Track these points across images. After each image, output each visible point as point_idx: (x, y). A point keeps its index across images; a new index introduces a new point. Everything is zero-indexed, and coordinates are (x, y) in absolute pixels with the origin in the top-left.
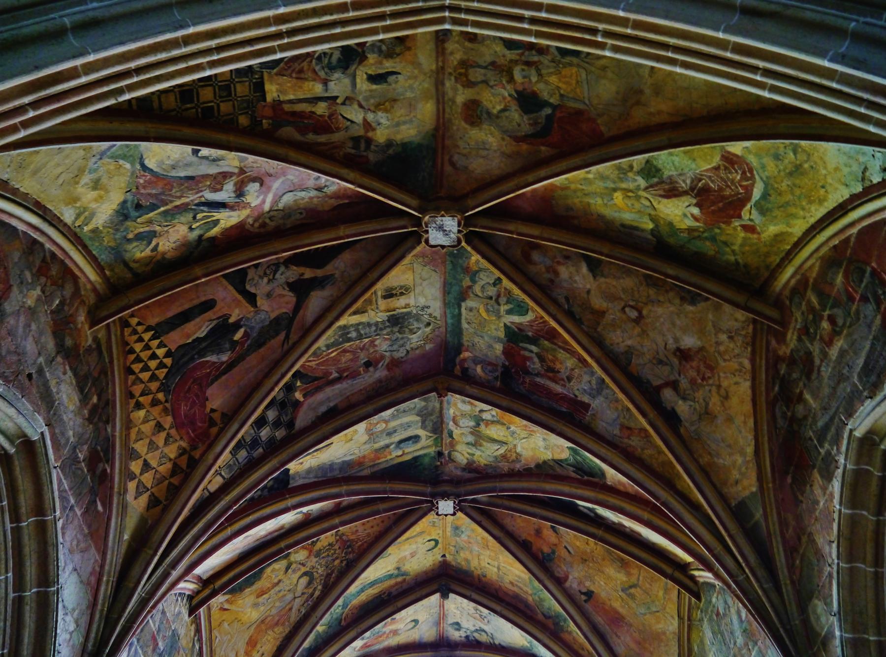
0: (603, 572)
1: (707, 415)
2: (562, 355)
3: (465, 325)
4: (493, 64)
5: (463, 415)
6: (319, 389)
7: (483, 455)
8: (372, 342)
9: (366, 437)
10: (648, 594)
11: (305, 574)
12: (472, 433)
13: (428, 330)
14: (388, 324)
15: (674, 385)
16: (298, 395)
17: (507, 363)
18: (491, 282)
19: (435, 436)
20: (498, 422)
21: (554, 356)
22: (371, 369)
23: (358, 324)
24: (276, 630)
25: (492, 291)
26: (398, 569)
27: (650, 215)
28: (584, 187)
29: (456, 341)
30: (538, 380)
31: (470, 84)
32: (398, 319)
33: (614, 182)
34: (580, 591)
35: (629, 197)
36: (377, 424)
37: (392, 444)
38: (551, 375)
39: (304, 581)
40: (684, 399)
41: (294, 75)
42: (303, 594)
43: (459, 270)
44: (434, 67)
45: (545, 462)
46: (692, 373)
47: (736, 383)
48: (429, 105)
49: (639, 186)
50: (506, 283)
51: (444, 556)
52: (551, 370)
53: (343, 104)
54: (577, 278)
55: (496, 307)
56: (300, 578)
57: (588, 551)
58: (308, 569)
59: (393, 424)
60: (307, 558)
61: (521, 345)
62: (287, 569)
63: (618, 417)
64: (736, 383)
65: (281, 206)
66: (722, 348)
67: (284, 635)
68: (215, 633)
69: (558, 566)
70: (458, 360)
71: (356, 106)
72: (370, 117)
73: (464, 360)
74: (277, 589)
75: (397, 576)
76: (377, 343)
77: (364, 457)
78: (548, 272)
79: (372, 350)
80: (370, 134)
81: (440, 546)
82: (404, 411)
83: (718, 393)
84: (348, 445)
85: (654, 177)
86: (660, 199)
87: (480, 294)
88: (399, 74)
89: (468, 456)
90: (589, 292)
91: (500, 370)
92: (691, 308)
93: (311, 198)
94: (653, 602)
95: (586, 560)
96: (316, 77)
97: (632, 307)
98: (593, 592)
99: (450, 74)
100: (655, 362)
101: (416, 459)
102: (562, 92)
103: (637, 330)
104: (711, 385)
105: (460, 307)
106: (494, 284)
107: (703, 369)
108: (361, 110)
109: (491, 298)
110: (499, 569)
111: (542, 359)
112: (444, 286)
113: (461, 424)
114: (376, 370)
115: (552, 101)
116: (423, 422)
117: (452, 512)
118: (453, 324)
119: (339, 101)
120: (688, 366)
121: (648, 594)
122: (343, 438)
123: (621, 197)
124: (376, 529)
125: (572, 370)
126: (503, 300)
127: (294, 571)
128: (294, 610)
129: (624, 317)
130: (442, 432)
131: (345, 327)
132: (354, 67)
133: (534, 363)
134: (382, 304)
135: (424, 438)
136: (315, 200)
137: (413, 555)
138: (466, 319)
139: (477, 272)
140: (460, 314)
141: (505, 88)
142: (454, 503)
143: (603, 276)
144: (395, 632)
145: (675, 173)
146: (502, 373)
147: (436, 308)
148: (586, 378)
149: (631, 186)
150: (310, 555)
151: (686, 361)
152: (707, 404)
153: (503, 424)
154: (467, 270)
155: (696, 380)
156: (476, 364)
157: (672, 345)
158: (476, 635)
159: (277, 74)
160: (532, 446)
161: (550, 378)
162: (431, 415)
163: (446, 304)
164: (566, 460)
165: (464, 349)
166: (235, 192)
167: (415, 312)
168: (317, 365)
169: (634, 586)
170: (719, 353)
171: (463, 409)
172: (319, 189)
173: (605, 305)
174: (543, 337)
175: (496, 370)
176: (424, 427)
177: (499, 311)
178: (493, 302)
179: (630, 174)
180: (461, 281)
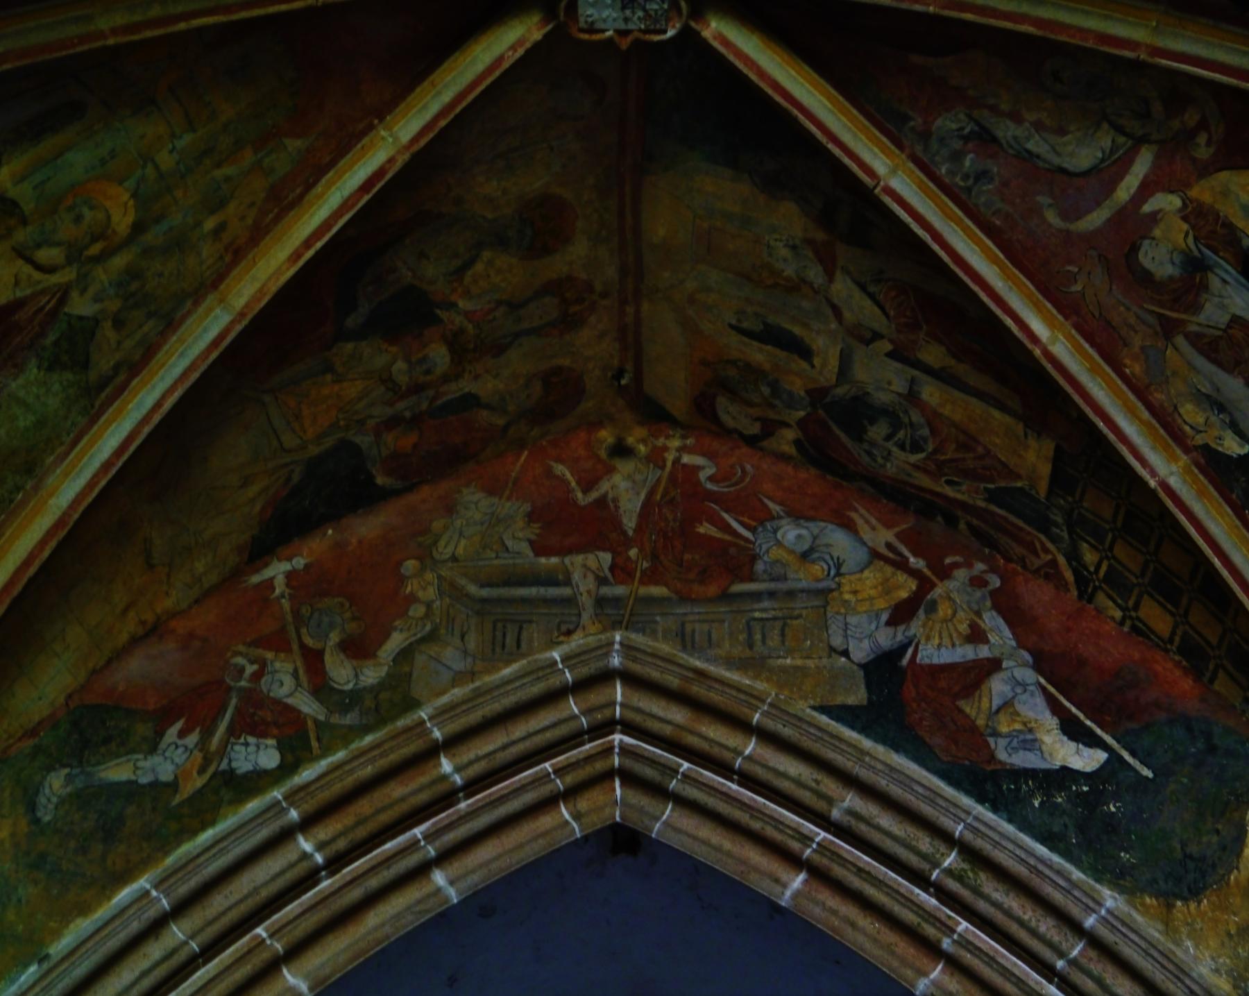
4: (499, 350)
27: (24, 222)
28: (218, 173)
31: (555, 288)
33: (147, 252)
35: (95, 239)
41: (980, 450)
44: (645, 306)
48: (662, 232)
49: (83, 291)
53: (876, 336)
65: (1105, 139)
71: (847, 315)
72: (815, 274)
80: (820, 236)
85: (56, 343)
86: (19, 294)
88: (731, 326)
93: (1017, 118)
96: (933, 418)
99: (604, 295)
102: (329, 377)
108: (836, 301)
115: (350, 346)
119: (889, 347)
123: (116, 218)
132: (840, 391)
136: (1004, 107)
141: (467, 314)
145: (14, 385)
149: (102, 276)
159: (1019, 477)
166: (1204, 287)
172: (985, 139)
179: (113, 306)
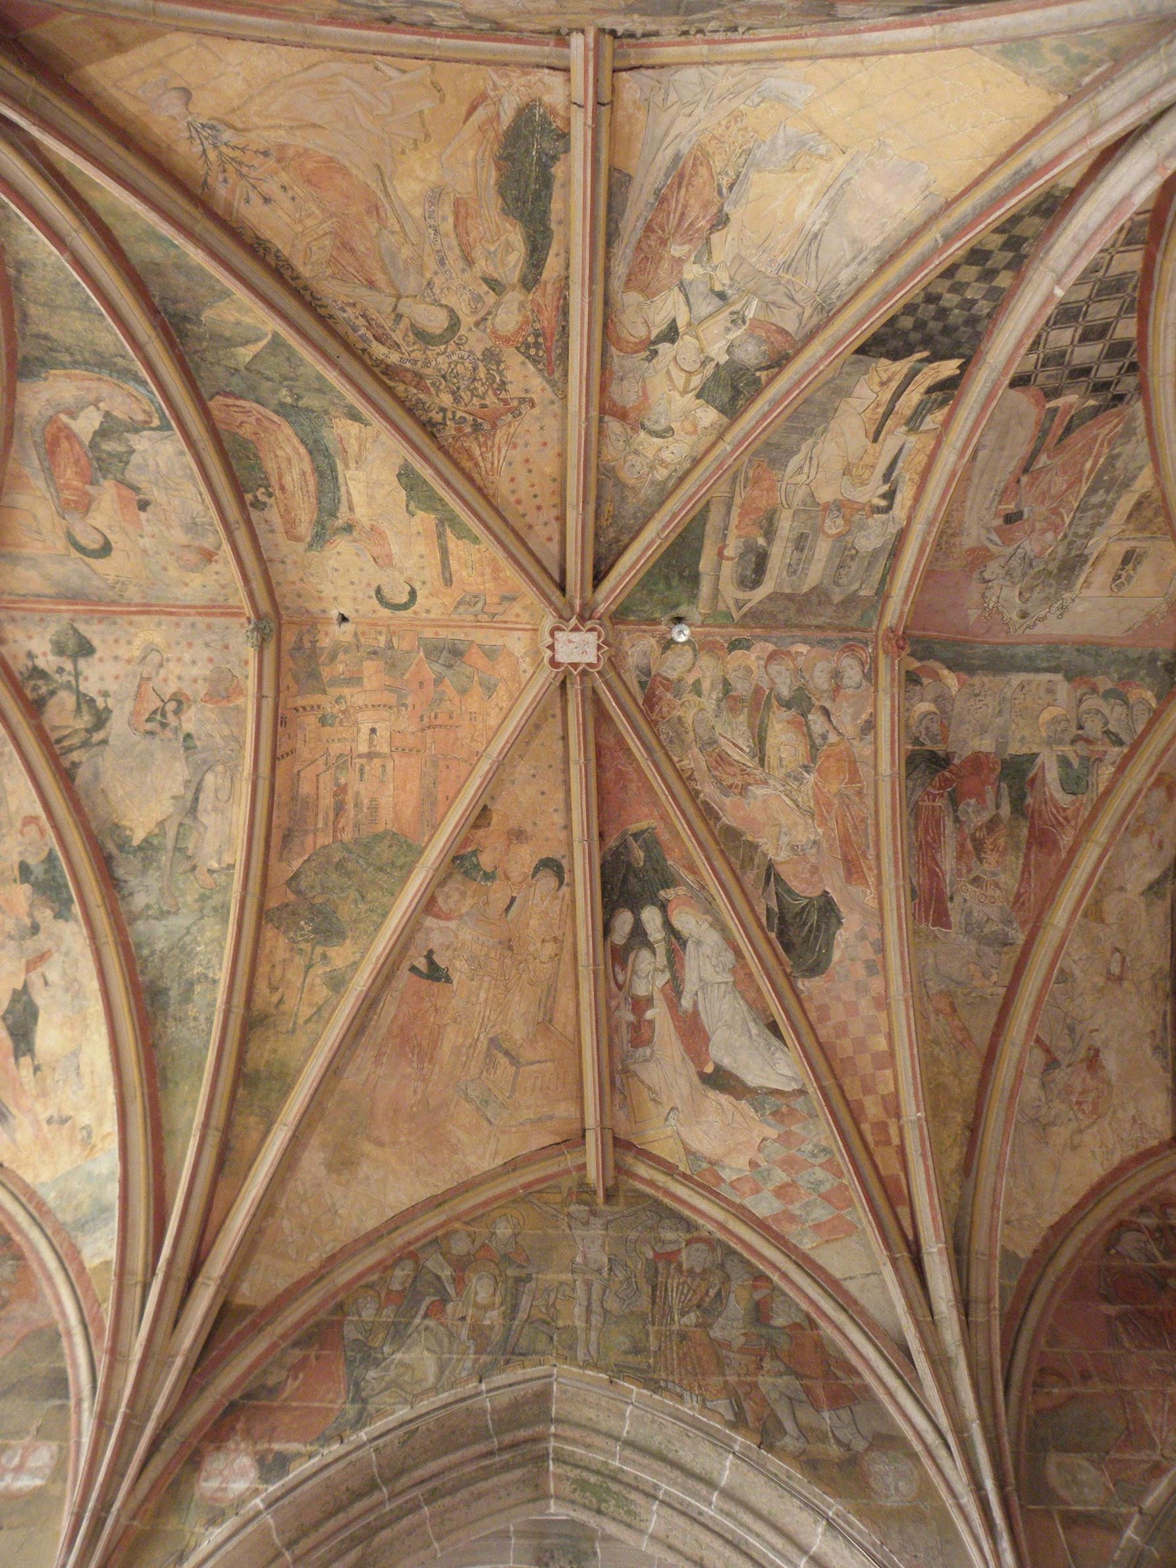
0: (508, 990)
1: (1043, 1127)
2: (1015, 862)
3: (1016, 679)
5: (798, 672)
6: (1044, 432)
7: (710, 714)
8: (1056, 529)
9: (826, 495)
10: (513, 1090)
11: (455, 323)
12: (758, 690)
13: (1014, 616)
14: (1074, 553)
15: (1052, 1063)
16: (1070, 400)
17: (956, 761)
18: (1110, 726)
19: (736, 616)
20: (813, 745)
21: (1005, 848)
22: (999, 522)
23: (1111, 510)
24: (327, 242)
25: (1094, 728)
26: (349, 528)
29: (977, 662)
30: (949, 825)
32: (1072, 569)
34: (431, 952)
36: (848, 522)
37: (770, 541)
38: (969, 846)
39: (436, 321)
40: (1043, 1085)
42: (399, 317)
43: (1126, 671)
45: (753, 847)
46: (1078, 1086)
47: (1093, 1153)
50: (1115, 752)
51: (344, 619)
52: (979, 846)
54: (1136, 866)
55: (1068, 737)
56: (452, 313)
57: (532, 948)
58: (463, 331)
59: (823, 549)
60: (494, 332)
61: (1003, 785)
62: (494, 285)
63: (959, 983)
64: (1093, 1153)
66: (1120, 1114)
67: (297, 261)
68: (421, 70)
69: (463, 894)
70: (931, 663)
73: (937, 677)
74: (453, 257)
75: (320, 523)
76: (1049, 536)
77: (771, 489)
78: (1137, 820)
79: (1038, 526)
81: (386, 612)
82: (841, 567)
83: (1073, 1133)
84: (838, 466)
87: (1084, 706)
89: (690, 679)
90: (1122, 889)
91: (939, 748)
92: (1149, 1051)
94: (503, 1106)
95: (510, 948)
97: (1123, 961)
98: (448, 980)
100: (1068, 1021)
101: (695, 579)
103: (1100, 981)
104: (1077, 1119)
105: (1055, 670)
106: (1107, 733)
107: (1091, 1097)
109: (1081, 727)
110: (370, 756)
111: (992, 824)
112: (1093, 643)
113: (774, 668)
114: (988, 530)
116: (790, 598)
117: (559, 658)
118: (1012, 657)
120: (1083, 1074)
121: (513, 1090)
122: (868, 460)
124: (504, 487)
125: (997, 885)
126: (1080, 747)
127: (478, 299)
128: (364, 292)
129: (1108, 954)
130: (744, 626)
131: (1126, 485)
133: (977, 813)
134: (1119, 550)
135: (741, 595)
137: (384, 561)
138: (1030, 682)
139: (1126, 703)
140: (1037, 670)
142: (590, 665)
143: (1148, 906)
144: (85, 506)
146: (932, 752)
147: (1054, 627)
148: (994, 912)
150: (498, 337)
151: (1089, 1068)
152: (1053, 1124)
153: (813, 759)
154: (1126, 680)
155: (1071, 1093)
156: (935, 701)
157: (1098, 1039)
158: (67, 699)
160: (782, 819)
161: (962, 846)
162: (800, 611)
163: (1054, 646)
164: (789, 891)
165: (964, 676)
167: (1067, 595)
168: (1097, 436)
169: (514, 1059)
170: (1114, 1113)
171: (817, 673)
173: (1110, 919)
174: (1032, 825)
175: (933, 738)
176: (771, 598)
177: (1061, 742)
178: (1074, 731)
180: (1106, 673)
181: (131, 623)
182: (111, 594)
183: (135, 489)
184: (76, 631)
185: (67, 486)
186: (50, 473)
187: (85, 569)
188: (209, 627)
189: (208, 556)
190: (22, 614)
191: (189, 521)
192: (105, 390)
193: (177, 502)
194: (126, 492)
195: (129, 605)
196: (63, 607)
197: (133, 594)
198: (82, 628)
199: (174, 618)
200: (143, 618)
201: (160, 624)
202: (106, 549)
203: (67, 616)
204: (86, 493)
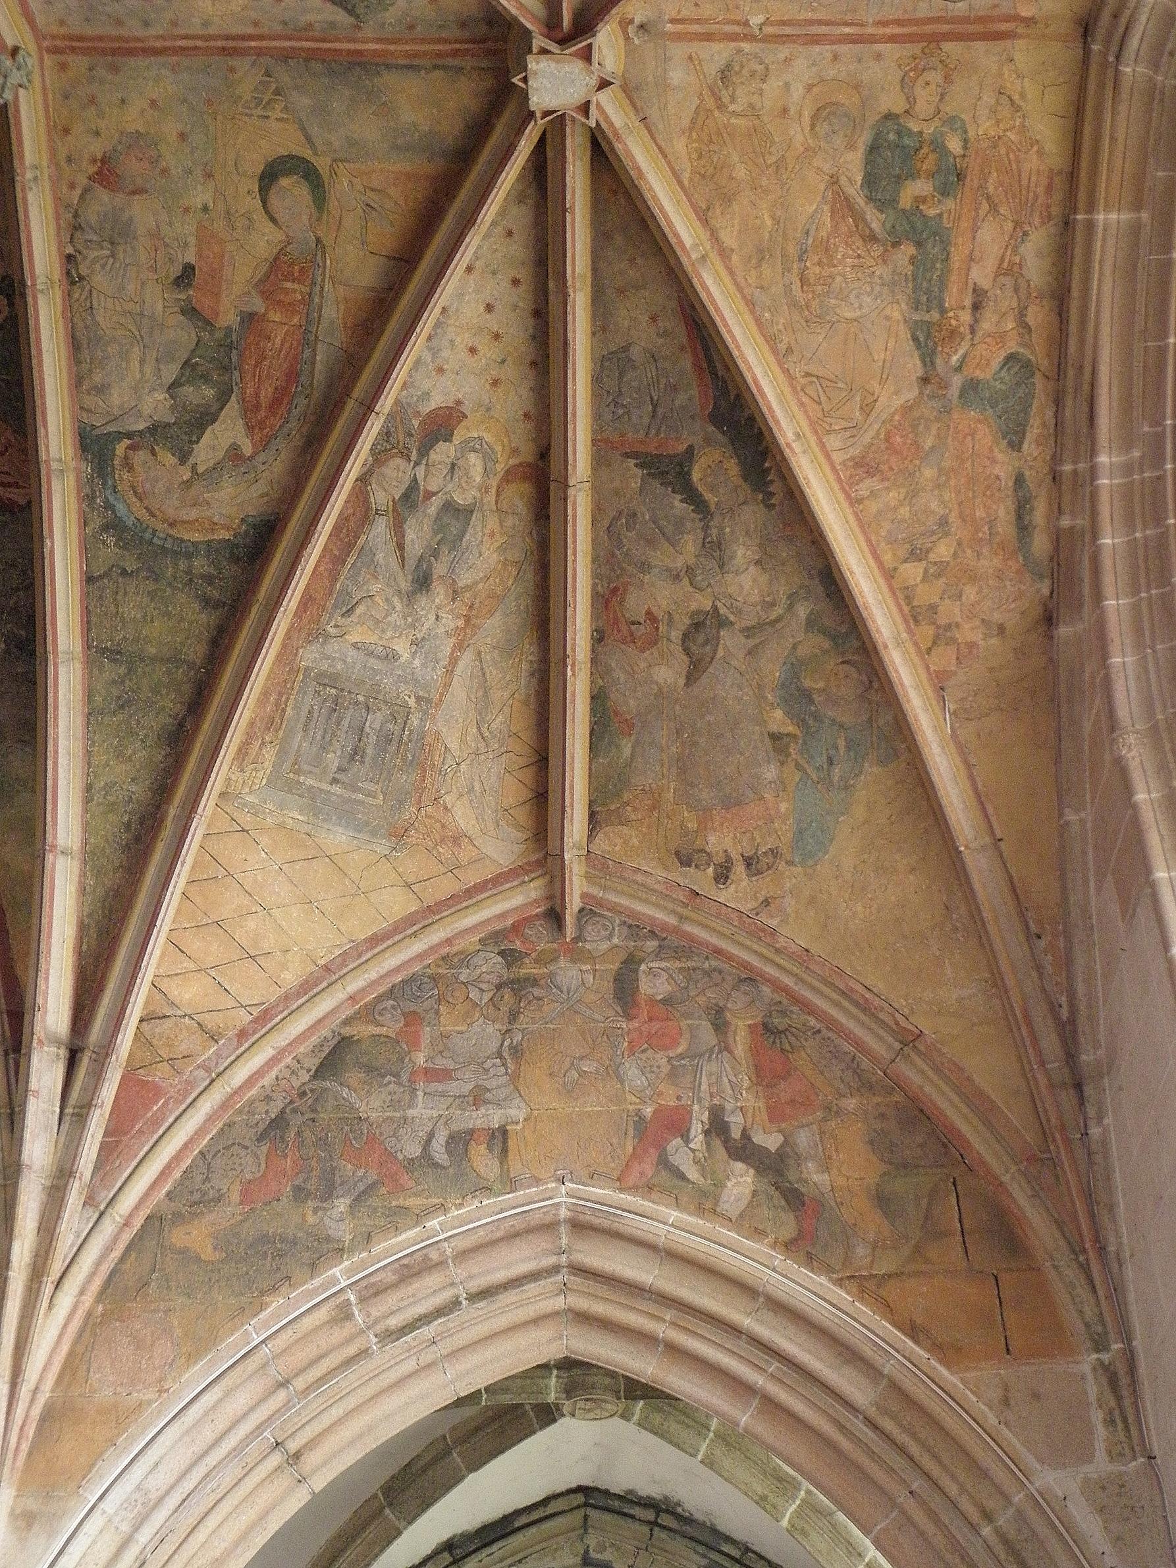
181: (256, 24)
182: (284, 76)
183: (191, 312)
184: (351, 12)
185: (290, 308)
186: (306, 338)
187: (314, 131)
188: (119, 22)
189: (106, 173)
190: (444, 35)
191: (121, 249)
192: (172, 507)
193: (131, 287)
194: (204, 303)
195: (260, 52)
196: (372, 46)
197: (247, 77)
198: (340, 16)
199: (182, 32)
200: (235, 30)
201: (205, 24)
202: (269, 177)
203: (368, 32)
204: (266, 295)
